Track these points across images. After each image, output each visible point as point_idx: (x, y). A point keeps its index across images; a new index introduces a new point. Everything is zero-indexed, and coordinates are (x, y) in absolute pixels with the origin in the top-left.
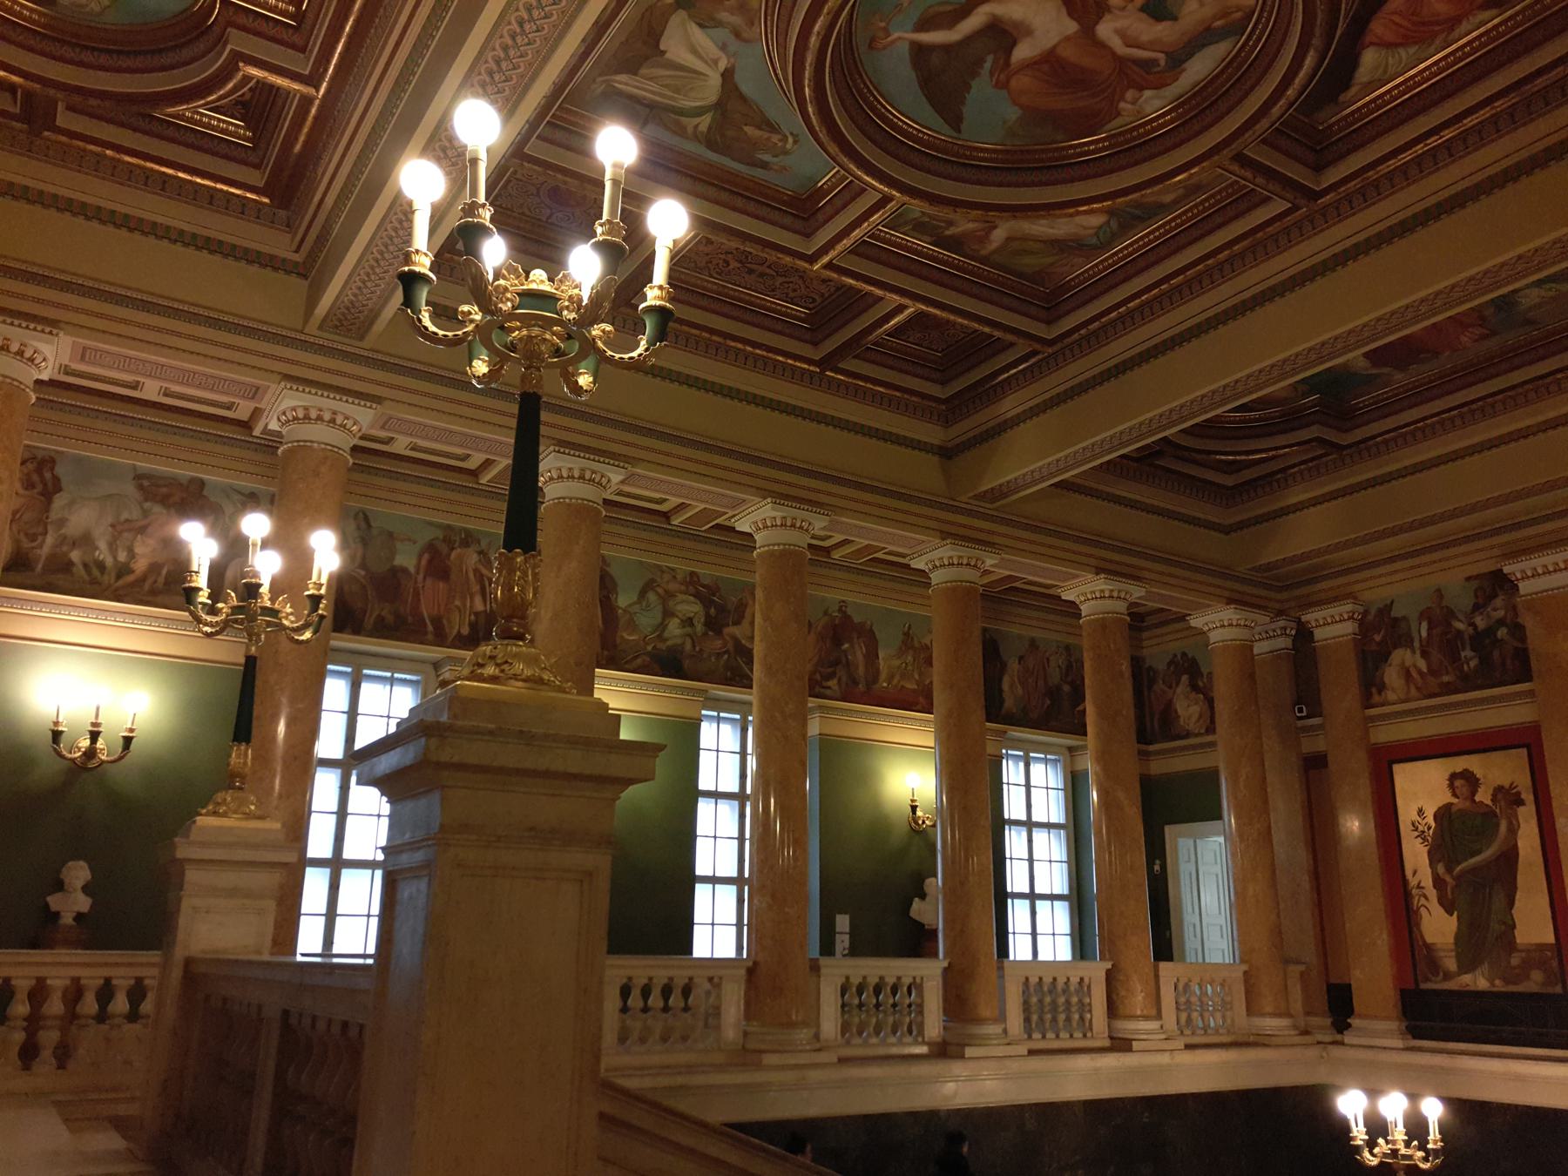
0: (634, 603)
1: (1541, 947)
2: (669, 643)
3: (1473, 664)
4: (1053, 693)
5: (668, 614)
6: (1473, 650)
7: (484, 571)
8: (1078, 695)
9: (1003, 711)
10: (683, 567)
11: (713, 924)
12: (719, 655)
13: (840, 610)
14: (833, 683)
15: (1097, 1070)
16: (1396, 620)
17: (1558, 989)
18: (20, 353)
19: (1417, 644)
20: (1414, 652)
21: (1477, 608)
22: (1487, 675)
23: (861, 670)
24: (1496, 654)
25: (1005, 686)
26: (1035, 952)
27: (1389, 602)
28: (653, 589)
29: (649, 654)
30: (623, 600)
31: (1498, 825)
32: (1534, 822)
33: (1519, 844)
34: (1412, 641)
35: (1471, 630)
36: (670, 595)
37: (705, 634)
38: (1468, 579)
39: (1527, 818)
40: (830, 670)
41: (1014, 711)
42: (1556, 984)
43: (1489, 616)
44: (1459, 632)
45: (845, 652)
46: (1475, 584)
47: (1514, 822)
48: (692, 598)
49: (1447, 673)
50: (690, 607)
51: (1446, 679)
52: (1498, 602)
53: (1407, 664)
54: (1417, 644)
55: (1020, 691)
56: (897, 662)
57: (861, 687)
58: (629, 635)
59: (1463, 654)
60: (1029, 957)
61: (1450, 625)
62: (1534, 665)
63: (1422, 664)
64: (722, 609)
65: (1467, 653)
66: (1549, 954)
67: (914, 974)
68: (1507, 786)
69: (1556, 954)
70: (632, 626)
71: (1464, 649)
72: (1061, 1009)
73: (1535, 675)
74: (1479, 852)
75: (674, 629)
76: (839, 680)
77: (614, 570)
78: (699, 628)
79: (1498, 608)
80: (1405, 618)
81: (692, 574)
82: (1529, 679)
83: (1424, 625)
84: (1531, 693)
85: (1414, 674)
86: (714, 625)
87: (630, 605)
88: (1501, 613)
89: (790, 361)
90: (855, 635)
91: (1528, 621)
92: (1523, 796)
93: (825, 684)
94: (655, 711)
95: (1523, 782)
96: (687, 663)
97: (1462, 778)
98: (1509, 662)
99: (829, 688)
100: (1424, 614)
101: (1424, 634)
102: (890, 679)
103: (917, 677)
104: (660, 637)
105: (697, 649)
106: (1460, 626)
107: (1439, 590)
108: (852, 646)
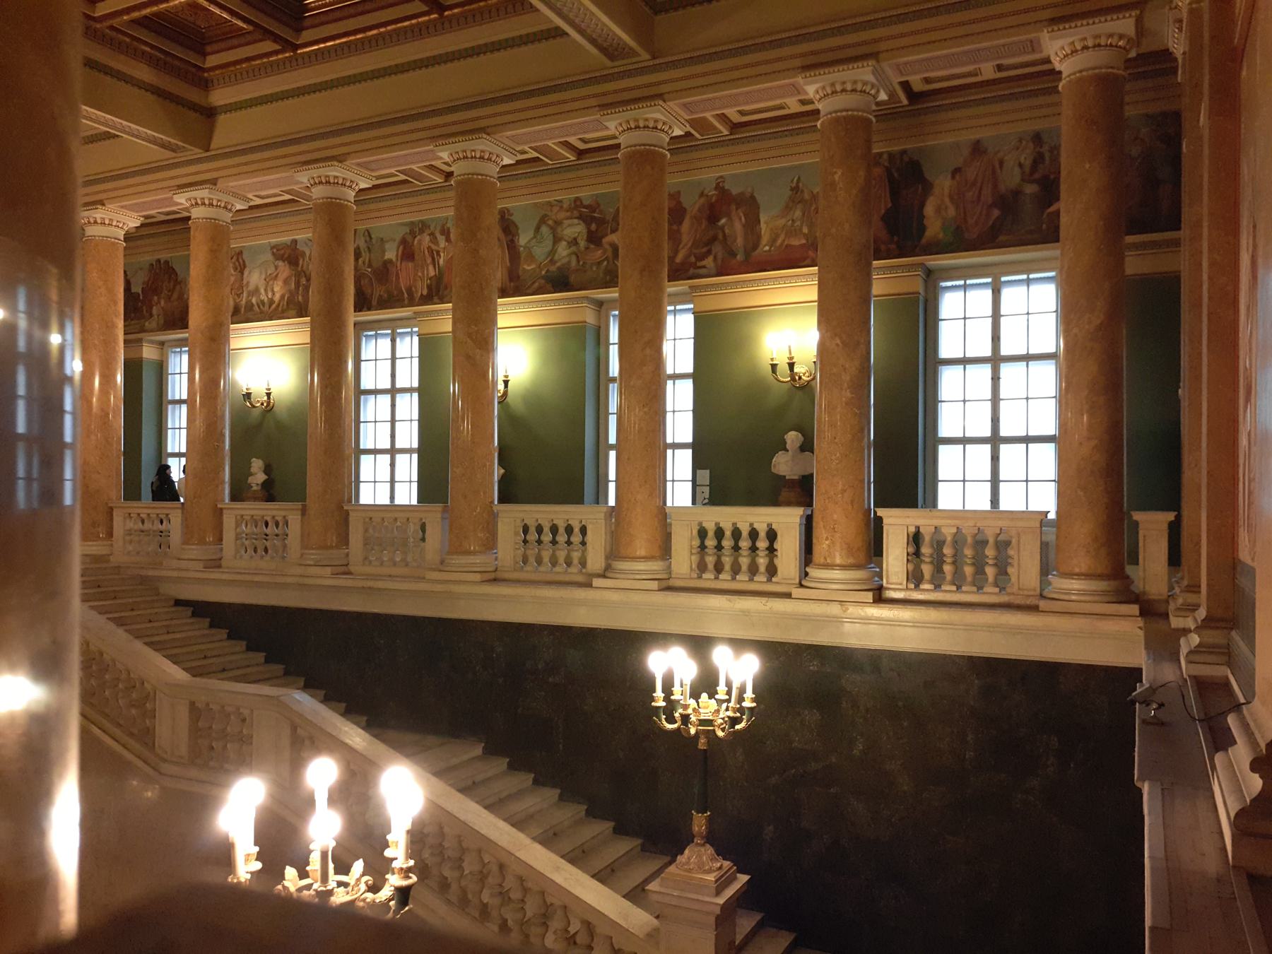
0: (532, 239)
2: (558, 264)
4: (1008, 203)
5: (556, 240)
7: (434, 247)
8: (1049, 190)
9: (924, 241)
10: (567, 197)
11: (964, 481)
12: (599, 263)
13: (717, 187)
14: (709, 262)
15: (746, 613)
18: (95, 222)
23: (740, 241)
25: (929, 209)
26: (392, 497)
28: (545, 223)
29: (543, 277)
30: (523, 240)
36: (558, 223)
37: (587, 248)
40: (705, 250)
41: (941, 236)
45: (722, 228)
48: (576, 221)
50: (575, 229)
55: (952, 212)
56: (781, 222)
57: (740, 257)
58: (528, 266)
60: (987, 506)
64: (601, 222)
67: (580, 517)
70: (531, 257)
72: (949, 560)
75: (563, 251)
76: (715, 257)
77: (516, 218)
78: (582, 244)
81: (577, 199)
86: (594, 239)
87: (529, 241)
89: (322, 45)
90: (733, 207)
93: (699, 264)
94: (546, 322)
96: (572, 279)
99: (704, 267)
102: (772, 242)
103: (805, 230)
104: (552, 262)
105: (581, 263)
108: (730, 219)
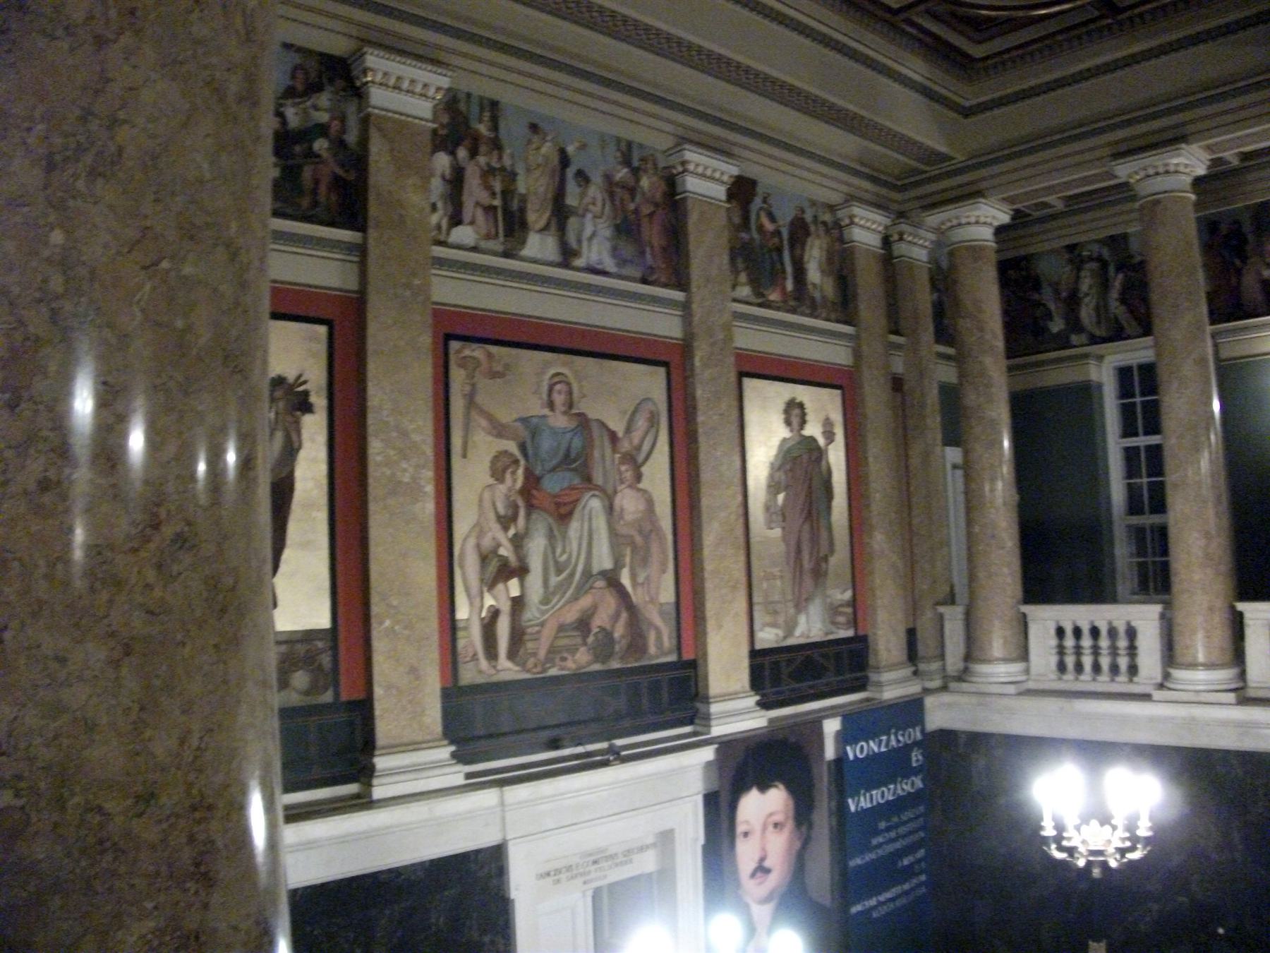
1: (309, 636)
17: (327, 697)
21: (290, 93)
24: (307, 173)
32: (322, 438)
33: (298, 473)
39: (314, 429)
42: (326, 689)
43: (305, 111)
46: (298, 59)
47: (294, 437)
52: (324, 99)
66: (320, 644)
68: (291, 376)
69: (329, 644)
88: (323, 117)
91: (377, 147)
92: (313, 399)
95: (315, 378)
98: (323, 189)
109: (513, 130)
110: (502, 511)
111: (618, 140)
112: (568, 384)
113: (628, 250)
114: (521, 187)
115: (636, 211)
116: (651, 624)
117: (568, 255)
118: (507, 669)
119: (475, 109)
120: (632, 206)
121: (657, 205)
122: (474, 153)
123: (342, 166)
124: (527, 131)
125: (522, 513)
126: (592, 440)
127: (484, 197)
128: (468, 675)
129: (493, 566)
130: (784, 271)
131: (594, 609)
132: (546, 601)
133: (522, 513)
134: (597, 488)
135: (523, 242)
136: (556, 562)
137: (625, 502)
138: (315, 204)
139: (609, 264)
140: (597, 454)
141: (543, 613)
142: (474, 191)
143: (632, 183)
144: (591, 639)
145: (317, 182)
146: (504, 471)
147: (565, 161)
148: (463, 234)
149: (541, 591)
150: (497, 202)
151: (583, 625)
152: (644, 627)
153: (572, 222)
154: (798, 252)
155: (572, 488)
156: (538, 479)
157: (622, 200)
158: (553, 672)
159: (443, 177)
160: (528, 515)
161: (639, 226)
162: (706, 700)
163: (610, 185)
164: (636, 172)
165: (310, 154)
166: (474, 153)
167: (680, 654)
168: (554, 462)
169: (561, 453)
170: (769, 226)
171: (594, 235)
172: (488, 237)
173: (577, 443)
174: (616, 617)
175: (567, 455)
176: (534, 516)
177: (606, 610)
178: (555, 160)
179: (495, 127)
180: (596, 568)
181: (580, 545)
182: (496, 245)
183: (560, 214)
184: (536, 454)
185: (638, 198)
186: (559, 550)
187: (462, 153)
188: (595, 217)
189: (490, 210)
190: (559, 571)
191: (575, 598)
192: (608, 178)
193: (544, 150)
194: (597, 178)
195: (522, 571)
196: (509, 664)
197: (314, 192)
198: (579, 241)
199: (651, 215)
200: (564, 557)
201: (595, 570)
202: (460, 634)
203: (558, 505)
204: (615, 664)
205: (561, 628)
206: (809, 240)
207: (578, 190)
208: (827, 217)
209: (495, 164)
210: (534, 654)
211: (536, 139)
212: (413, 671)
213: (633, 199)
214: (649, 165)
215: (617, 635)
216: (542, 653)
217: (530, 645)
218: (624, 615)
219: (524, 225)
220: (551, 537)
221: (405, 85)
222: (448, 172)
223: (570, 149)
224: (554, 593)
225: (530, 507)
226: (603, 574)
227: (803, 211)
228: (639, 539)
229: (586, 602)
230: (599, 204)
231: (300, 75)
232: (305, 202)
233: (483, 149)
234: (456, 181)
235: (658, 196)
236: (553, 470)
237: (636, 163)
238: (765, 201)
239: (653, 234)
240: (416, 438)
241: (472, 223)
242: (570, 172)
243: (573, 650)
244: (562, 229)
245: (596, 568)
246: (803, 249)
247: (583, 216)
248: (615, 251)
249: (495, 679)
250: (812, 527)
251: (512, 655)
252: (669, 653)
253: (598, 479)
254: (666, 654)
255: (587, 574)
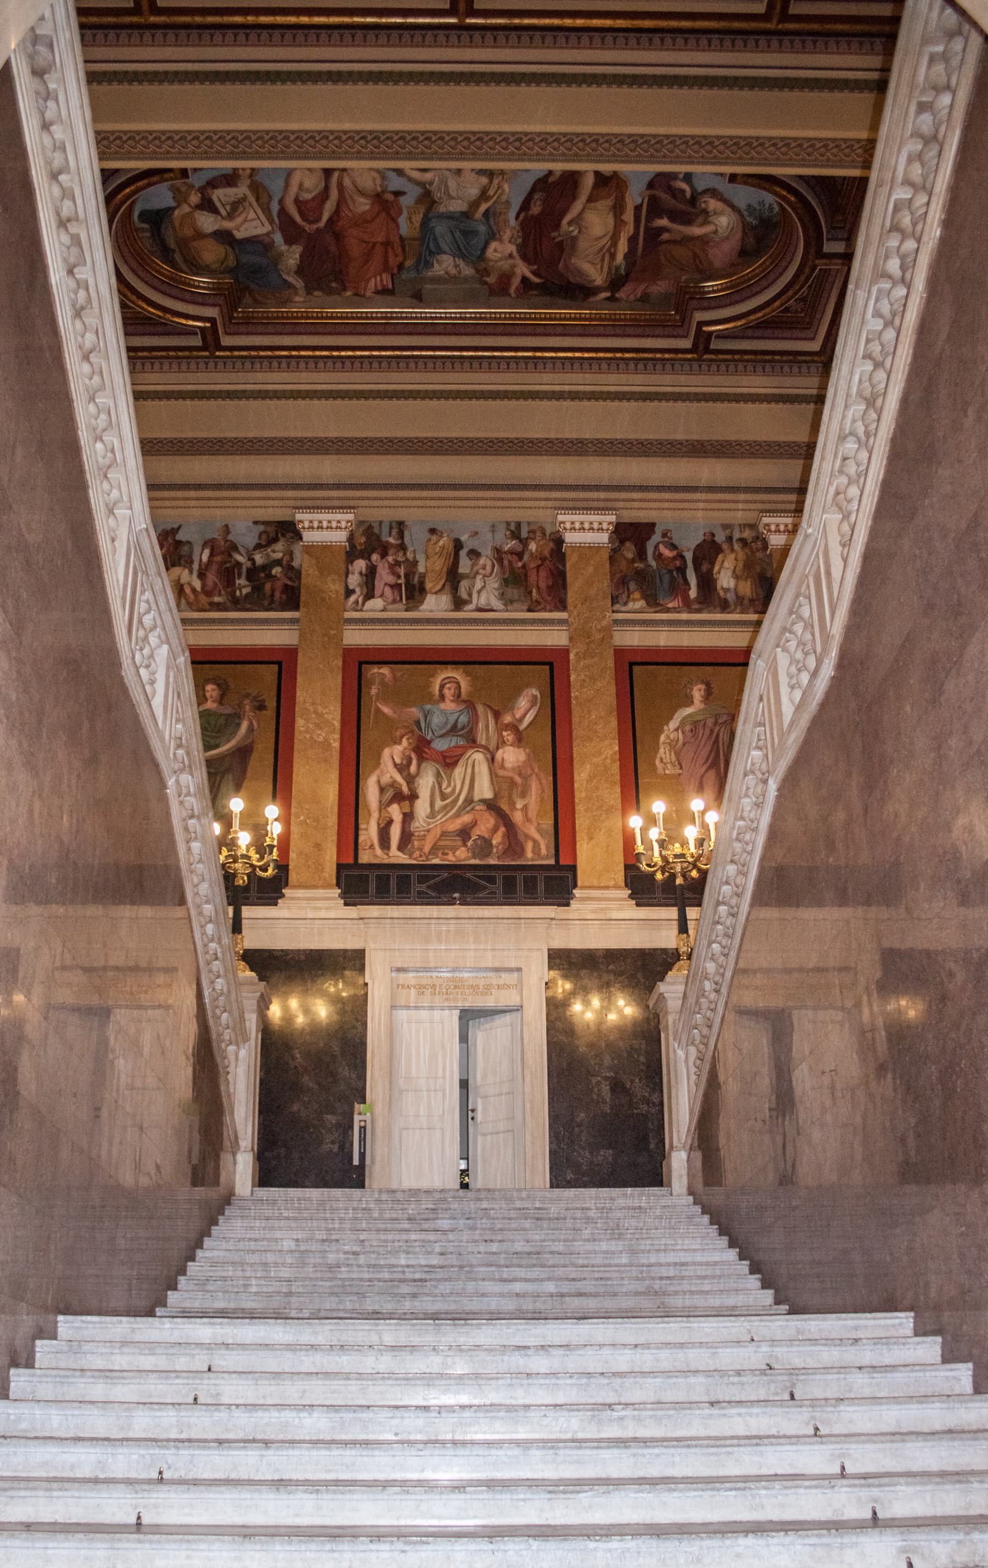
3: (245, 591)
6: (249, 578)
16: (179, 544)
19: (196, 566)
20: (191, 572)
21: (258, 547)
22: (257, 600)
24: (268, 587)
27: (176, 526)
31: (239, 725)
34: (192, 562)
35: (249, 564)
38: (256, 523)
43: (268, 555)
44: (239, 564)
46: (262, 528)
49: (220, 595)
51: (217, 599)
52: (279, 546)
53: (182, 581)
54: (196, 566)
59: (237, 582)
61: (230, 556)
62: (303, 598)
63: (197, 584)
65: (241, 581)
71: (239, 577)
73: (301, 605)
74: (217, 746)
79: (278, 551)
80: (188, 543)
82: (297, 608)
83: (207, 553)
84: (293, 621)
85: (188, 590)
88: (279, 555)
97: (215, 684)
100: (210, 543)
101: (205, 558)
106: (239, 558)
107: (227, 526)
109: (416, 538)
110: (398, 761)
111: (508, 524)
112: (458, 683)
113: (513, 592)
114: (421, 568)
115: (524, 566)
116: (527, 836)
117: (459, 604)
118: (396, 856)
119: (385, 529)
120: (520, 564)
121: (543, 559)
122: (384, 555)
123: (290, 579)
124: (428, 535)
125: (414, 762)
126: (477, 715)
127: (391, 579)
128: (364, 858)
129: (389, 794)
130: (687, 583)
131: (474, 824)
132: (432, 815)
133: (414, 762)
134: (482, 746)
135: (422, 602)
136: (441, 791)
137: (506, 757)
138: (272, 601)
139: (496, 603)
140: (481, 725)
141: (429, 824)
142: (384, 576)
143: (519, 548)
144: (469, 843)
145: (273, 590)
146: (402, 737)
147: (458, 545)
148: (376, 603)
149: (428, 810)
150: (402, 581)
151: (464, 833)
152: (521, 838)
153: (464, 584)
154: (705, 567)
155: (457, 747)
156: (429, 742)
157: (510, 562)
158: (436, 861)
159: (361, 574)
160: (419, 766)
161: (526, 575)
162: (575, 886)
163: (499, 554)
164: (524, 542)
165: (270, 576)
166: (384, 555)
167: (557, 861)
168: (442, 732)
169: (449, 726)
170: (667, 553)
171: (484, 587)
172: (394, 602)
173: (463, 719)
174: (495, 830)
175: (455, 726)
176: (424, 765)
177: (486, 824)
178: (451, 546)
179: (401, 535)
180: (477, 797)
181: (463, 783)
182: (400, 606)
183: (453, 578)
184: (428, 725)
185: (526, 557)
186: (444, 786)
187: (375, 557)
188: (484, 576)
189: (395, 587)
190: (444, 797)
191: (458, 815)
192: (498, 551)
193: (441, 543)
194: (487, 552)
195: (413, 797)
196: (400, 854)
197: (272, 595)
198: (470, 595)
199: (538, 568)
200: (449, 790)
201: (476, 798)
202: (361, 832)
203: (445, 758)
204: (492, 861)
205: (444, 834)
206: (720, 557)
207: (469, 563)
208: (747, 534)
209: (400, 559)
210: (421, 849)
211: (434, 538)
212: (318, 846)
213: (521, 558)
214: (539, 534)
215: (494, 842)
216: (427, 849)
217: (416, 843)
218: (502, 829)
219: (422, 591)
220: (438, 776)
221: (325, 524)
222: (364, 570)
223: (464, 538)
224: (439, 812)
225: (421, 759)
226: (483, 801)
227: (713, 535)
228: (518, 780)
229: (466, 818)
230: (489, 568)
231: (264, 537)
232: (266, 603)
233: (391, 552)
234: (371, 574)
235: (546, 553)
236: (442, 736)
237: (524, 534)
238: (664, 535)
239: (541, 580)
240: (329, 717)
241: (382, 596)
242: (463, 553)
243: (454, 849)
244: (455, 589)
245: (477, 797)
246: (713, 564)
247: (474, 577)
248: (502, 596)
249: (386, 861)
250: (718, 774)
251: (400, 848)
252: (547, 857)
253: (481, 739)
254: (542, 859)
255: (469, 801)
